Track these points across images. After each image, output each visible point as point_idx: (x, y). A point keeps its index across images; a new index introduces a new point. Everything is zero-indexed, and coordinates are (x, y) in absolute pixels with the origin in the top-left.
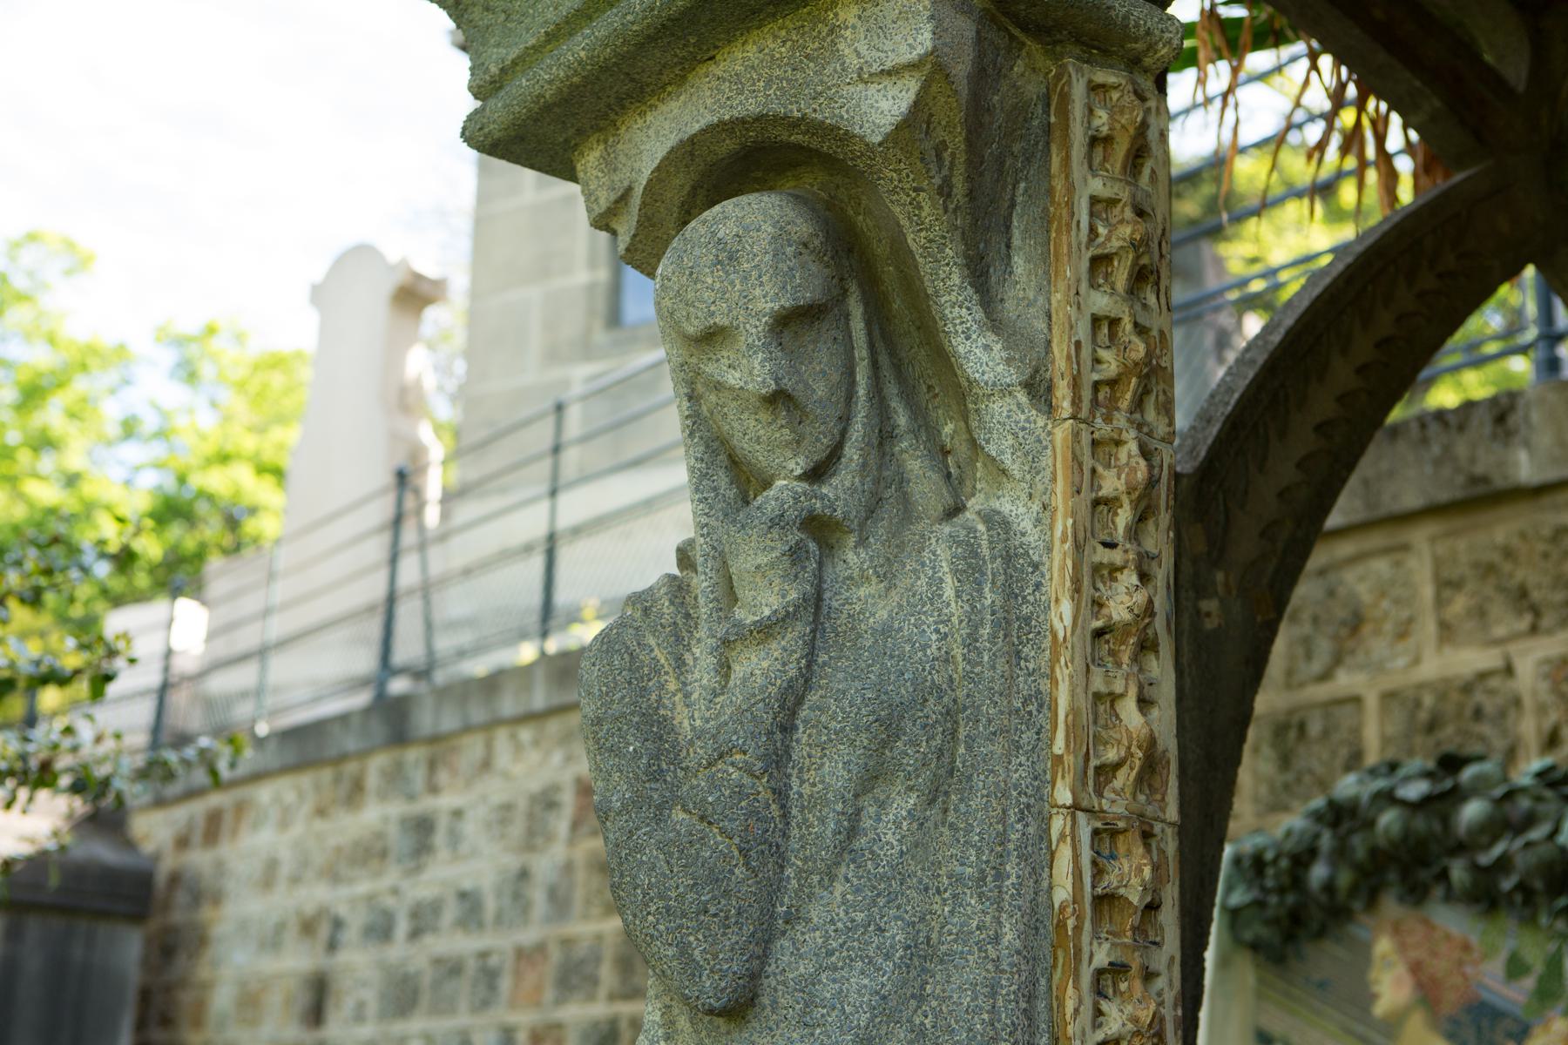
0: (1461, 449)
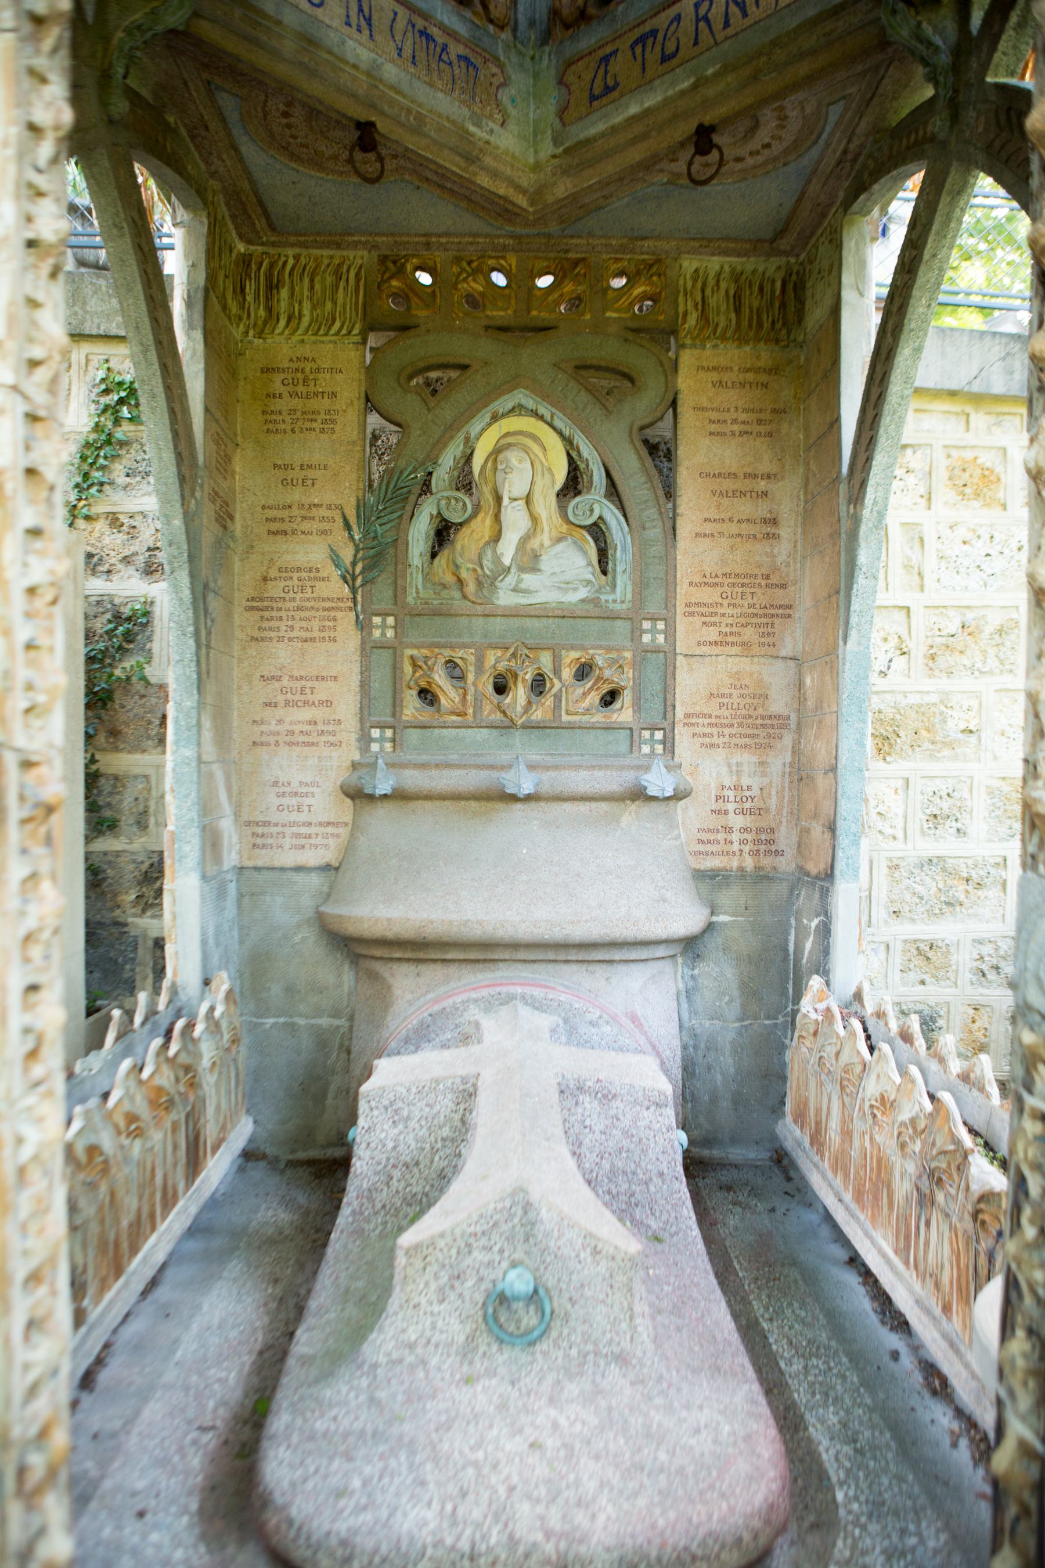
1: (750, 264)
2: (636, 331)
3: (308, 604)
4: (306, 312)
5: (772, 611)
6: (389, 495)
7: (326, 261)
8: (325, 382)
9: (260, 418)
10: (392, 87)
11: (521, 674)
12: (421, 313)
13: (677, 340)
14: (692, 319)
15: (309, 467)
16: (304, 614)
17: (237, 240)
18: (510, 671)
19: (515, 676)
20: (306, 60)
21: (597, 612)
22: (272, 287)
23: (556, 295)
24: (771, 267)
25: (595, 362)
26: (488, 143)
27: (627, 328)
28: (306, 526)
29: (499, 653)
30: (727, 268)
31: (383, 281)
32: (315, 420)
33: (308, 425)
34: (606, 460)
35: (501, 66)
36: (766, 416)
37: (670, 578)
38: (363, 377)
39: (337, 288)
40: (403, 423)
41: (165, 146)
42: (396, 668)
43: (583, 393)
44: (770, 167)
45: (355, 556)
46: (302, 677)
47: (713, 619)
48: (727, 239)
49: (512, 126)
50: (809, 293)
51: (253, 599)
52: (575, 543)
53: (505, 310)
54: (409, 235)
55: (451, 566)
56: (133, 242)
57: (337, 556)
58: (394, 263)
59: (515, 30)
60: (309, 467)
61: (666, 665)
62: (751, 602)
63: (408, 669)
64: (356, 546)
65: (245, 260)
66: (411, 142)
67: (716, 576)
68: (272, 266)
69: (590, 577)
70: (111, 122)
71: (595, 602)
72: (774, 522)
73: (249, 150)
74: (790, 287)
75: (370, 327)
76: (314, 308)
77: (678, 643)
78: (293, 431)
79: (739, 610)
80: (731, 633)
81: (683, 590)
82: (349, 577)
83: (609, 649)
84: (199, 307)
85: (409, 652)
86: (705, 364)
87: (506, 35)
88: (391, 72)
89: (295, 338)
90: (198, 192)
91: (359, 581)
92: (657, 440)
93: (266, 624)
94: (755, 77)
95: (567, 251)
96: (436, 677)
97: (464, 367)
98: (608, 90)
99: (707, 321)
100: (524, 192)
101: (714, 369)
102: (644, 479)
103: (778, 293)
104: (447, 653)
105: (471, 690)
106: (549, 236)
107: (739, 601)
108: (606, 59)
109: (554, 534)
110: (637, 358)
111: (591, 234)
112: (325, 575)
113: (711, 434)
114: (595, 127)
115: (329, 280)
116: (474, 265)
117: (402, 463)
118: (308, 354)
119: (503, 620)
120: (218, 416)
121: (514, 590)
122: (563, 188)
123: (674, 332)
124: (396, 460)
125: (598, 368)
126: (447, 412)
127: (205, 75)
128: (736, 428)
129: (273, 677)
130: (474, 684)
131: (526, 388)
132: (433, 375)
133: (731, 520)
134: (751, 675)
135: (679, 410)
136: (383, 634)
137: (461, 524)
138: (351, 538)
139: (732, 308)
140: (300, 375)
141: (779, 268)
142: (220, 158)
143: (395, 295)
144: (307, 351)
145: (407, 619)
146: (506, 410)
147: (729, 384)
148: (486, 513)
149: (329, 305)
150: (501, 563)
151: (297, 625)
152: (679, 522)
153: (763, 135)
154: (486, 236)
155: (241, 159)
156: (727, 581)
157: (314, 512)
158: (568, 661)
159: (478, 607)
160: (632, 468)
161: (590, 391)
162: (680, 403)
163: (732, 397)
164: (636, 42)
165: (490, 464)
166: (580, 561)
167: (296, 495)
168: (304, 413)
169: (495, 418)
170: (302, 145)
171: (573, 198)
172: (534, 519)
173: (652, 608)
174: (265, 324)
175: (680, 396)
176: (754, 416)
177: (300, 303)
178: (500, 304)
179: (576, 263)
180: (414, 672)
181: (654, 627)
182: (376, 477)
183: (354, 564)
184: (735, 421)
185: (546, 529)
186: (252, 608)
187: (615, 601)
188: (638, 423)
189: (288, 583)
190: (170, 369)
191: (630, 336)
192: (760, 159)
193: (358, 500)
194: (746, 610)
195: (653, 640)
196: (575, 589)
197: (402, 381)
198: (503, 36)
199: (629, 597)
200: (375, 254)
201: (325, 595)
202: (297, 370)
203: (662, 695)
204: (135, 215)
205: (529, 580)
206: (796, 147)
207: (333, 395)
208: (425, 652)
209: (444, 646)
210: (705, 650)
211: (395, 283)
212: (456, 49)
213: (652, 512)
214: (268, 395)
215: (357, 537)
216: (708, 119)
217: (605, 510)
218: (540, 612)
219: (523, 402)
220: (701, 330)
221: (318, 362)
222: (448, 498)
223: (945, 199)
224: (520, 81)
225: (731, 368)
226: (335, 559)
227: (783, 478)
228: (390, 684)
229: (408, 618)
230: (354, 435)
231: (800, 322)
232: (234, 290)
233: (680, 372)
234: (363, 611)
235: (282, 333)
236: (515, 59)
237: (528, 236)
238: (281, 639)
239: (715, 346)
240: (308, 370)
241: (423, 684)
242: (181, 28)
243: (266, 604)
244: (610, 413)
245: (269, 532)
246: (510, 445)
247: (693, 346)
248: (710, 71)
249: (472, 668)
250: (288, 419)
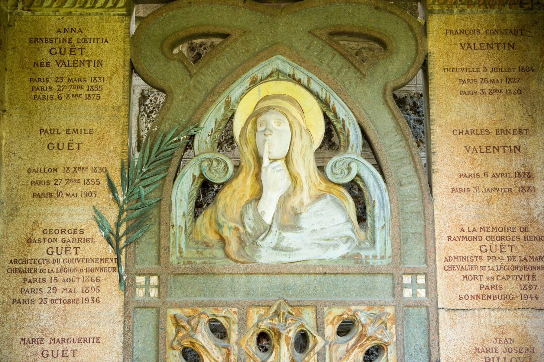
3: (71, 266)
5: (532, 263)
6: (153, 158)
8: (91, 51)
9: (28, 85)
11: (284, 333)
13: (425, 7)
15: (75, 131)
16: (67, 275)
18: (273, 329)
19: (279, 335)
21: (358, 268)
25: (347, 29)
28: (71, 188)
29: (262, 311)
32: (81, 87)
33: (74, 91)
34: (362, 121)
36: (514, 74)
37: (429, 233)
38: (128, 46)
40: (165, 87)
42: (159, 328)
45: (119, 217)
46: (63, 340)
47: (473, 273)
51: (16, 261)
52: (334, 200)
55: (214, 224)
57: (102, 217)
60: (75, 131)
61: (428, 319)
62: (510, 254)
63: (171, 329)
64: (121, 208)
67: (474, 230)
69: (350, 233)
71: (356, 258)
72: (529, 175)
77: (440, 298)
78: (60, 97)
79: (499, 263)
80: (493, 287)
81: (441, 243)
82: (112, 238)
83: (371, 306)
85: (172, 312)
86: (453, 28)
89: (63, 11)
91: (123, 242)
92: (404, 95)
93: (29, 286)
96: (199, 337)
97: (225, 36)
101: (462, 32)
102: (398, 137)
104: (210, 312)
105: (235, 349)
107: (498, 254)
109: (314, 192)
112: (89, 236)
113: (462, 93)
117: (165, 127)
118: (75, 25)
119: (265, 277)
121: (276, 248)
124: (160, 125)
125: (351, 34)
126: (208, 77)
128: (485, 86)
129: (34, 340)
130: (238, 343)
131: (283, 54)
132: (198, 41)
133: (486, 175)
134: (516, 328)
135: (430, 71)
136: (147, 294)
137: (223, 184)
138: (116, 199)
140: (67, 45)
145: (171, 278)
146: (265, 75)
147: (477, 46)
148: (247, 174)
150: (262, 221)
151: (60, 286)
152: (435, 178)
156: (484, 235)
157: (79, 175)
158: (331, 317)
159: (241, 266)
160: (387, 127)
161: (344, 56)
162: (430, 64)
163: (480, 58)
165: (250, 126)
166: (340, 218)
167: (61, 159)
168: (70, 80)
169: (254, 83)
172: (294, 178)
173: (412, 263)
175: (430, 58)
176: (503, 75)
180: (178, 332)
181: (414, 282)
182: (144, 133)
183: (118, 225)
184: (484, 80)
185: (306, 187)
186: (15, 271)
187: (375, 257)
188: (391, 85)
189: (51, 245)
193: (123, 163)
194: (505, 263)
195: (414, 295)
196: (336, 246)
197: (165, 49)
199: (389, 252)
201: (89, 256)
202: (64, 40)
203: (425, 350)
205: (291, 238)
207: (99, 63)
208: (188, 311)
209: (207, 306)
210: (467, 303)
213: (408, 169)
214: (36, 64)
215: (121, 199)
217: (363, 168)
218: (302, 270)
221: (85, 32)
222: (210, 160)
225: (478, 31)
226: (99, 220)
227: (535, 133)
228: (154, 344)
229: (170, 275)
230: (119, 100)
233: (430, 36)
234: (127, 272)
235: (50, 6)
238: (43, 301)
239: (462, 11)
240: (74, 40)
241: (186, 344)
243: (29, 266)
244: (364, 76)
245: (34, 195)
246: (269, 108)
247: (441, 12)
249: (235, 327)
250: (55, 86)
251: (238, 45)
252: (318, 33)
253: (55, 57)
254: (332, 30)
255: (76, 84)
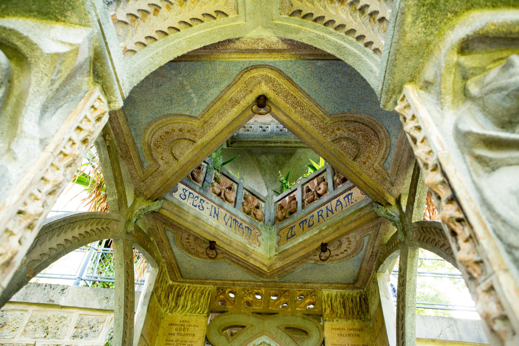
0: (51, 294)
1: (347, 292)
2: (308, 315)
4: (189, 305)
7: (199, 288)
8: (191, 330)
10: (222, 232)
12: (229, 307)
14: (328, 311)
17: (169, 280)
20: (195, 222)
22: (179, 296)
23: (278, 302)
24: (355, 293)
25: (292, 326)
26: (253, 250)
27: (304, 314)
30: (339, 293)
31: (217, 296)
35: (259, 230)
38: (206, 329)
39: (201, 297)
41: (147, 245)
43: (288, 338)
44: (348, 258)
48: (337, 283)
49: (262, 246)
50: (369, 301)
53: (260, 307)
54: (227, 280)
56: (125, 270)
58: (222, 290)
59: (264, 222)
65: (171, 287)
66: (227, 248)
68: (180, 289)
70: (127, 233)
73: (175, 250)
74: (362, 300)
75: (211, 311)
76: (192, 303)
84: (149, 298)
86: (334, 327)
87: (261, 223)
88: (223, 228)
89: (183, 314)
90: (157, 261)
94: (338, 229)
95: (282, 287)
97: (244, 327)
98: (292, 236)
99: (334, 312)
100: (266, 266)
103: (358, 302)
106: (275, 282)
108: (292, 228)
110: (308, 325)
111: (290, 282)
114: (288, 245)
115: (199, 294)
116: (250, 291)
118: (187, 320)
120: (147, 339)
122: (279, 265)
123: (321, 316)
127: (164, 226)
139: (342, 307)
140: (183, 327)
141: (358, 293)
142: (166, 252)
143: (221, 301)
144: (186, 318)
147: (344, 335)
149: (197, 303)
153: (344, 247)
154: (254, 281)
155: (173, 253)
162: (326, 342)
164: (301, 223)
168: (182, 341)
170: (192, 249)
171: (282, 268)
174: (174, 308)
175: (326, 340)
177: (187, 302)
178: (258, 305)
179: (285, 291)
190: (129, 316)
191: (305, 317)
192: (344, 255)
197: (220, 331)
198: (260, 223)
200: (216, 287)
204: (129, 261)
206: (356, 251)
207: (194, 335)
211: (221, 296)
212: (244, 225)
214: (169, 334)
216: (324, 241)
219: (265, 341)
220: (332, 314)
221: (190, 323)
223: (409, 260)
224: (265, 235)
231: (368, 312)
232: (165, 296)
233: (325, 330)
236: (264, 229)
237: (268, 282)
239: (337, 321)
240: (186, 325)
242: (157, 211)
248: (324, 228)
251: (249, 330)
252: (280, 327)
253: (177, 332)
254: (286, 326)
255: (183, 343)
